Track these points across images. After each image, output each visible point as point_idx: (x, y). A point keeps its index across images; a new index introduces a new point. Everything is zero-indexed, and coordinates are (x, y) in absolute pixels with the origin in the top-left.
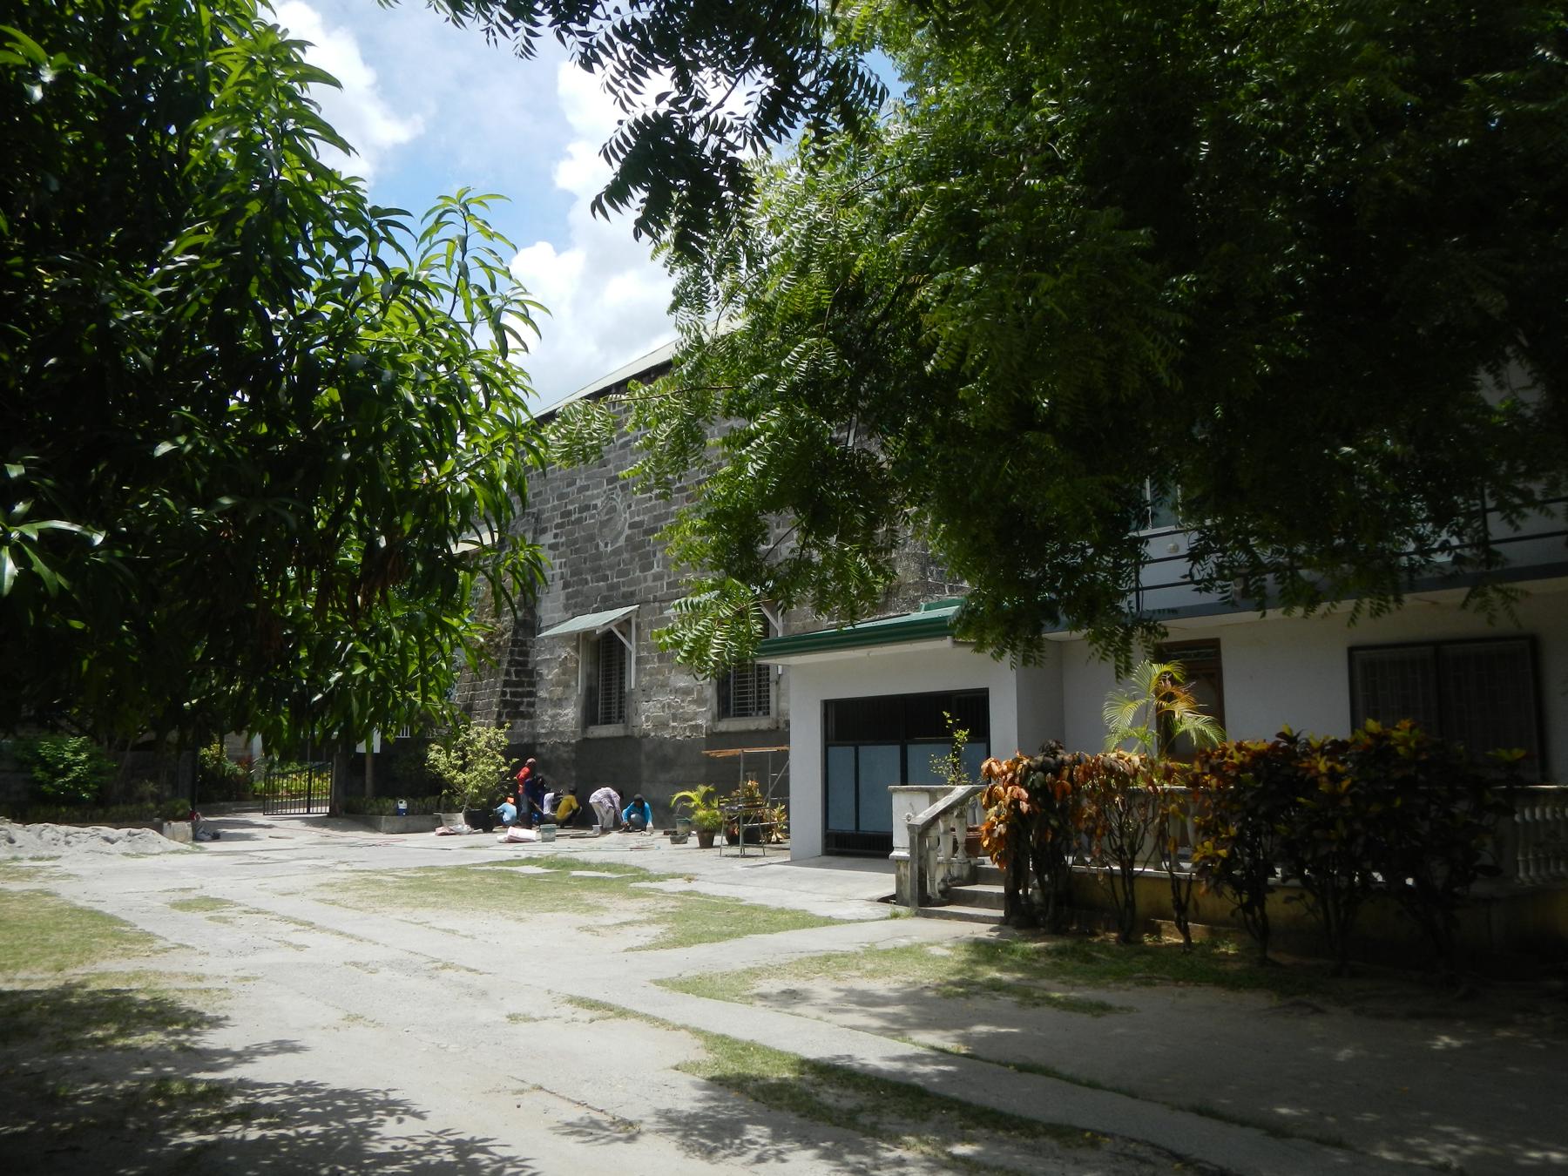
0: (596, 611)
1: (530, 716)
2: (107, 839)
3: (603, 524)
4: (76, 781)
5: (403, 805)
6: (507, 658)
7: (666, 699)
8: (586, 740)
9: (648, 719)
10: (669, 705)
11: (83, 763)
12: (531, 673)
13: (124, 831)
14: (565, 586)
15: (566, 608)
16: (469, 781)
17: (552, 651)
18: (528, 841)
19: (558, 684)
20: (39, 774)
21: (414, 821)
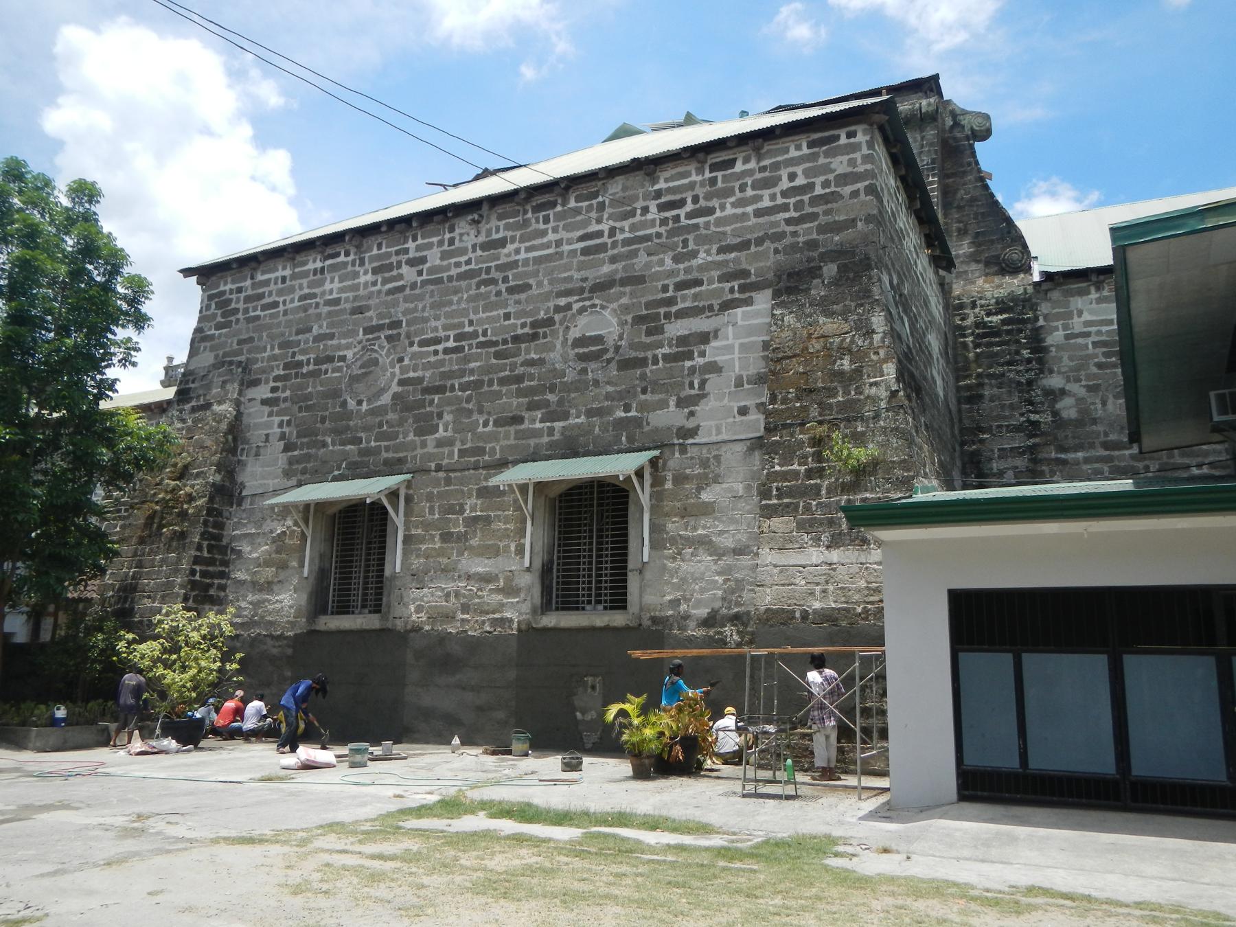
0: (335, 479)
3: (354, 379)
6: (200, 529)
7: (450, 586)
9: (419, 609)
10: (457, 594)
12: (223, 550)
14: (287, 449)
15: (287, 474)
17: (258, 524)
18: (328, 766)
19: (267, 563)
21: (75, 733)
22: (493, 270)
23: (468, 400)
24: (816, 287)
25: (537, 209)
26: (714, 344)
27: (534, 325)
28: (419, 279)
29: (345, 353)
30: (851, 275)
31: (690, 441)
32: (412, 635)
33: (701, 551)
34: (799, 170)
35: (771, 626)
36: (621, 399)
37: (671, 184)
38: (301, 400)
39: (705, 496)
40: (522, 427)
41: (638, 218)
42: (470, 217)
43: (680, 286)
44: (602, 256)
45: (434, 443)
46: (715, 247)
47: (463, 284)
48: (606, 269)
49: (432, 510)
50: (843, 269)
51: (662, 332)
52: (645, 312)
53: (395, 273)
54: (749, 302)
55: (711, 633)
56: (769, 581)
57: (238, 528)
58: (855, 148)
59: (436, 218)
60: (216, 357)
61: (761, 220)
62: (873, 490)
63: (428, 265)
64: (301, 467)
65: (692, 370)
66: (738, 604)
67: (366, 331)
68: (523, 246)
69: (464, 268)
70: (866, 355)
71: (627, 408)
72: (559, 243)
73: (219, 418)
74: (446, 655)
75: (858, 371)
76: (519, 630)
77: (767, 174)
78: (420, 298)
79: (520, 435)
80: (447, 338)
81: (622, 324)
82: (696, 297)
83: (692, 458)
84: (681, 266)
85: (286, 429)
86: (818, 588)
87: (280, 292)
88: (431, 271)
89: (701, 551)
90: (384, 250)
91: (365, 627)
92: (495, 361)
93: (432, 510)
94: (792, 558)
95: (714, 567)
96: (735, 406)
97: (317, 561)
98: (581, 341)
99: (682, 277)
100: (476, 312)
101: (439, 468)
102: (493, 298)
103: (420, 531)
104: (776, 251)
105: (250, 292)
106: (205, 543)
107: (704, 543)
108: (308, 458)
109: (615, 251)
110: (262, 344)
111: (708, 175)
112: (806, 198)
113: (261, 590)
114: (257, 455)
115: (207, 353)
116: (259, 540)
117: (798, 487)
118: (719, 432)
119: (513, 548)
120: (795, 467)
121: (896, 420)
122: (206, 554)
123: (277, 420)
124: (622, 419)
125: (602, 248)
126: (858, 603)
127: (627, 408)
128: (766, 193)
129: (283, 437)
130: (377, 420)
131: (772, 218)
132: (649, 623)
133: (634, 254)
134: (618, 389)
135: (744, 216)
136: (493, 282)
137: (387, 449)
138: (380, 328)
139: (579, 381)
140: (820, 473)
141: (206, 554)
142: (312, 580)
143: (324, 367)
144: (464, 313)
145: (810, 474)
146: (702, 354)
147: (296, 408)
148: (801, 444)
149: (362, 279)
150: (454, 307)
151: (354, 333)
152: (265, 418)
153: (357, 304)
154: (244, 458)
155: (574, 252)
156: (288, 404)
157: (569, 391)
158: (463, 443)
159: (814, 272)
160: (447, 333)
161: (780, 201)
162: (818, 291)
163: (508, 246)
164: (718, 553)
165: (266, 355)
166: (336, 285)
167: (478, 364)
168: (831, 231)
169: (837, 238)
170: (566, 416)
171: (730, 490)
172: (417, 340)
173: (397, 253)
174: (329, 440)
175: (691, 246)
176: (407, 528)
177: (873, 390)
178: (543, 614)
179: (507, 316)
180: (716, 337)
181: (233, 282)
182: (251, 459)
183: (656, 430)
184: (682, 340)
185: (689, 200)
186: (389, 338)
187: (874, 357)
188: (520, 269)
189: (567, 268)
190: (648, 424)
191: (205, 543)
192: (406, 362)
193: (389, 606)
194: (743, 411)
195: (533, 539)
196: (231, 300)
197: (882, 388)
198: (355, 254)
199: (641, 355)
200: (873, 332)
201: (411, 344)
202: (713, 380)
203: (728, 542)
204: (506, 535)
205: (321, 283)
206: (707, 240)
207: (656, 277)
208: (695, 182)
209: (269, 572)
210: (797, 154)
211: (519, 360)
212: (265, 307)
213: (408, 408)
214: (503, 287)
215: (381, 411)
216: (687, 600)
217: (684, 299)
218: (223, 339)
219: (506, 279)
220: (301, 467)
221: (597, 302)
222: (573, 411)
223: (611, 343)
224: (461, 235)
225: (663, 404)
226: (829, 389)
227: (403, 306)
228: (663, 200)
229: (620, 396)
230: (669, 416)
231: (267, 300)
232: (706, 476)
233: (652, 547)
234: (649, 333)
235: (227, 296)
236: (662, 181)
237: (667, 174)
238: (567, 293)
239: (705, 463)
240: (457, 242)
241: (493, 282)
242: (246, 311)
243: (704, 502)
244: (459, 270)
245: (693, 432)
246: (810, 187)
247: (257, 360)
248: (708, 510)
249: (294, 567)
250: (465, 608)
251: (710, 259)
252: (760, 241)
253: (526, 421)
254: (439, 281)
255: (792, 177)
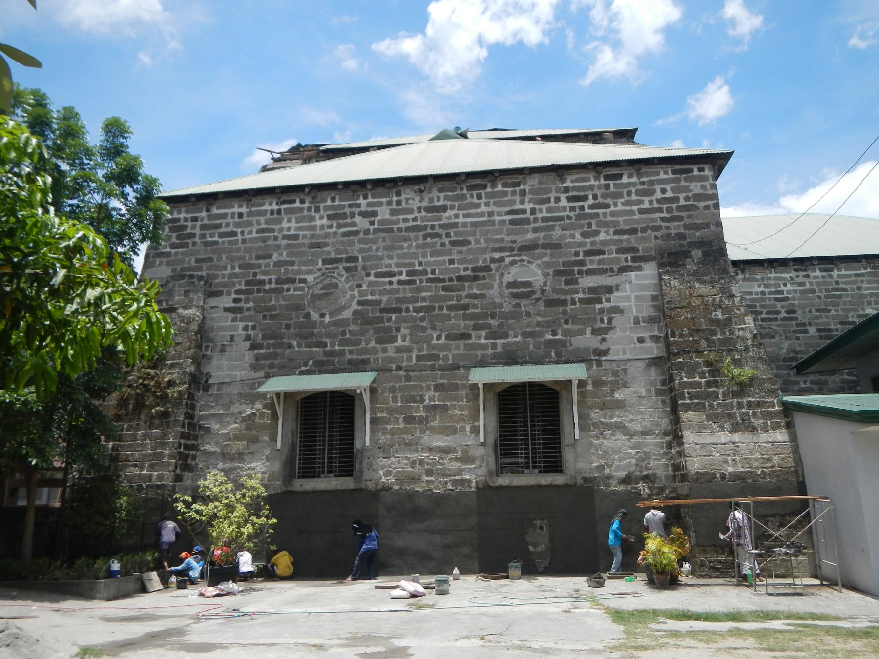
0: (302, 373)
3: (315, 298)
7: (415, 456)
10: (422, 462)
14: (253, 347)
15: (254, 367)
17: (227, 406)
19: (238, 438)
22: (437, 227)
23: (422, 319)
24: (690, 264)
25: (471, 188)
26: (616, 294)
27: (474, 269)
28: (372, 228)
29: (306, 277)
30: (712, 259)
31: (604, 358)
32: (383, 493)
33: (617, 432)
34: (668, 187)
35: (701, 483)
36: (550, 326)
37: (576, 184)
38: (266, 311)
39: (618, 396)
40: (470, 342)
41: (552, 204)
42: (417, 187)
43: (588, 253)
44: (526, 227)
45: (394, 350)
46: (612, 231)
47: (412, 235)
48: (530, 236)
49: (395, 399)
50: (705, 254)
51: (577, 284)
52: (562, 268)
53: (349, 220)
54: (639, 269)
55: (629, 488)
56: (694, 453)
57: (207, 410)
58: (705, 178)
59: (388, 185)
60: (174, 270)
61: (643, 216)
62: (753, 396)
63: (379, 218)
64: (267, 362)
65: (602, 311)
66: (647, 469)
67: (325, 262)
68: (461, 213)
69: (411, 223)
70: (732, 310)
71: (554, 333)
72: (491, 214)
73: (189, 321)
74: (412, 508)
75: (729, 320)
76: (477, 488)
77: (645, 187)
78: (375, 241)
79: (468, 347)
80: (401, 273)
81: (546, 275)
82: (600, 262)
83: (606, 370)
84: (588, 240)
85: (252, 333)
86: (729, 458)
87: (238, 225)
88: (381, 222)
89: (617, 432)
90: (337, 202)
91: (339, 487)
92: (443, 293)
93: (395, 399)
94: (707, 439)
95: (628, 444)
96: (635, 336)
97: (290, 436)
98: (513, 284)
99: (588, 247)
100: (424, 255)
101: (399, 368)
102: (439, 248)
103: (385, 415)
104: (656, 238)
105: (206, 222)
106: (186, 421)
107: (620, 427)
108: (275, 356)
109: (537, 225)
110: (222, 263)
111: (603, 182)
112: (674, 206)
113: (232, 459)
114: (223, 351)
115: (164, 267)
116: (227, 420)
117: (702, 392)
118: (624, 353)
119: (468, 428)
120: (697, 379)
121: (760, 353)
122: (187, 431)
123: (241, 325)
124: (550, 340)
125: (526, 221)
126: (757, 468)
127: (554, 333)
128: (646, 199)
129: (248, 338)
130: (340, 330)
131: (652, 216)
132: (582, 482)
133: (552, 228)
134: (547, 319)
135: (631, 212)
136: (438, 236)
137: (351, 352)
138: (339, 260)
139: (515, 312)
140: (716, 384)
141: (187, 431)
142: (286, 451)
143: (286, 286)
144: (415, 256)
145: (709, 384)
146: (608, 300)
147: (261, 316)
148: (698, 364)
149: (318, 222)
150: (404, 251)
151: (313, 262)
152: (229, 323)
153: (313, 241)
154: (209, 353)
155: (503, 222)
156: (252, 313)
157: (507, 318)
158: (419, 350)
159: (686, 254)
160: (400, 269)
161: (656, 205)
162: (691, 267)
163: (449, 211)
164: (630, 434)
165: (227, 272)
166: (293, 224)
167: (429, 294)
168: (693, 229)
169: (698, 234)
170: (506, 336)
171: (636, 392)
172: (373, 272)
173: (350, 206)
174: (295, 343)
175: (594, 227)
176: (373, 412)
177: (741, 333)
178: (497, 476)
179: (452, 262)
180: (617, 289)
181: (187, 212)
182: (216, 355)
183: (578, 349)
184: (592, 290)
185: (590, 197)
186: (347, 269)
187: (738, 312)
188: (460, 229)
189: (499, 232)
190: (571, 345)
191: (186, 421)
192: (364, 287)
193: (361, 472)
194: (641, 340)
195: (486, 420)
196: (186, 226)
197: (747, 332)
198: (311, 203)
199: (562, 297)
200: (734, 296)
201: (368, 275)
202: (617, 320)
203: (638, 428)
204: (461, 419)
205: (279, 221)
206: (606, 224)
207: (570, 245)
208: (594, 186)
209: (241, 445)
210: (665, 177)
211: (464, 294)
212: (221, 235)
213: (367, 322)
214: (447, 241)
215: (344, 323)
216: (610, 466)
217: (592, 262)
218: (179, 257)
219: (448, 235)
220: (267, 362)
221: (525, 258)
222: (511, 333)
223: (539, 288)
224: (407, 199)
225: (582, 332)
226: (711, 330)
227: (358, 246)
228: (570, 194)
229: (548, 324)
230: (587, 340)
231: (223, 230)
232: (617, 382)
233: (580, 429)
234: (567, 283)
235: (182, 222)
236: (569, 181)
237: (574, 177)
238: (501, 250)
239: (616, 373)
240: (403, 204)
241: (438, 236)
242: (203, 236)
243: (617, 400)
244: (407, 224)
245: (606, 352)
246: (675, 199)
247: (218, 276)
248: (620, 405)
249: (266, 441)
250: (429, 473)
251: (608, 237)
252: (644, 230)
253: (473, 338)
254: (391, 231)
255: (664, 191)
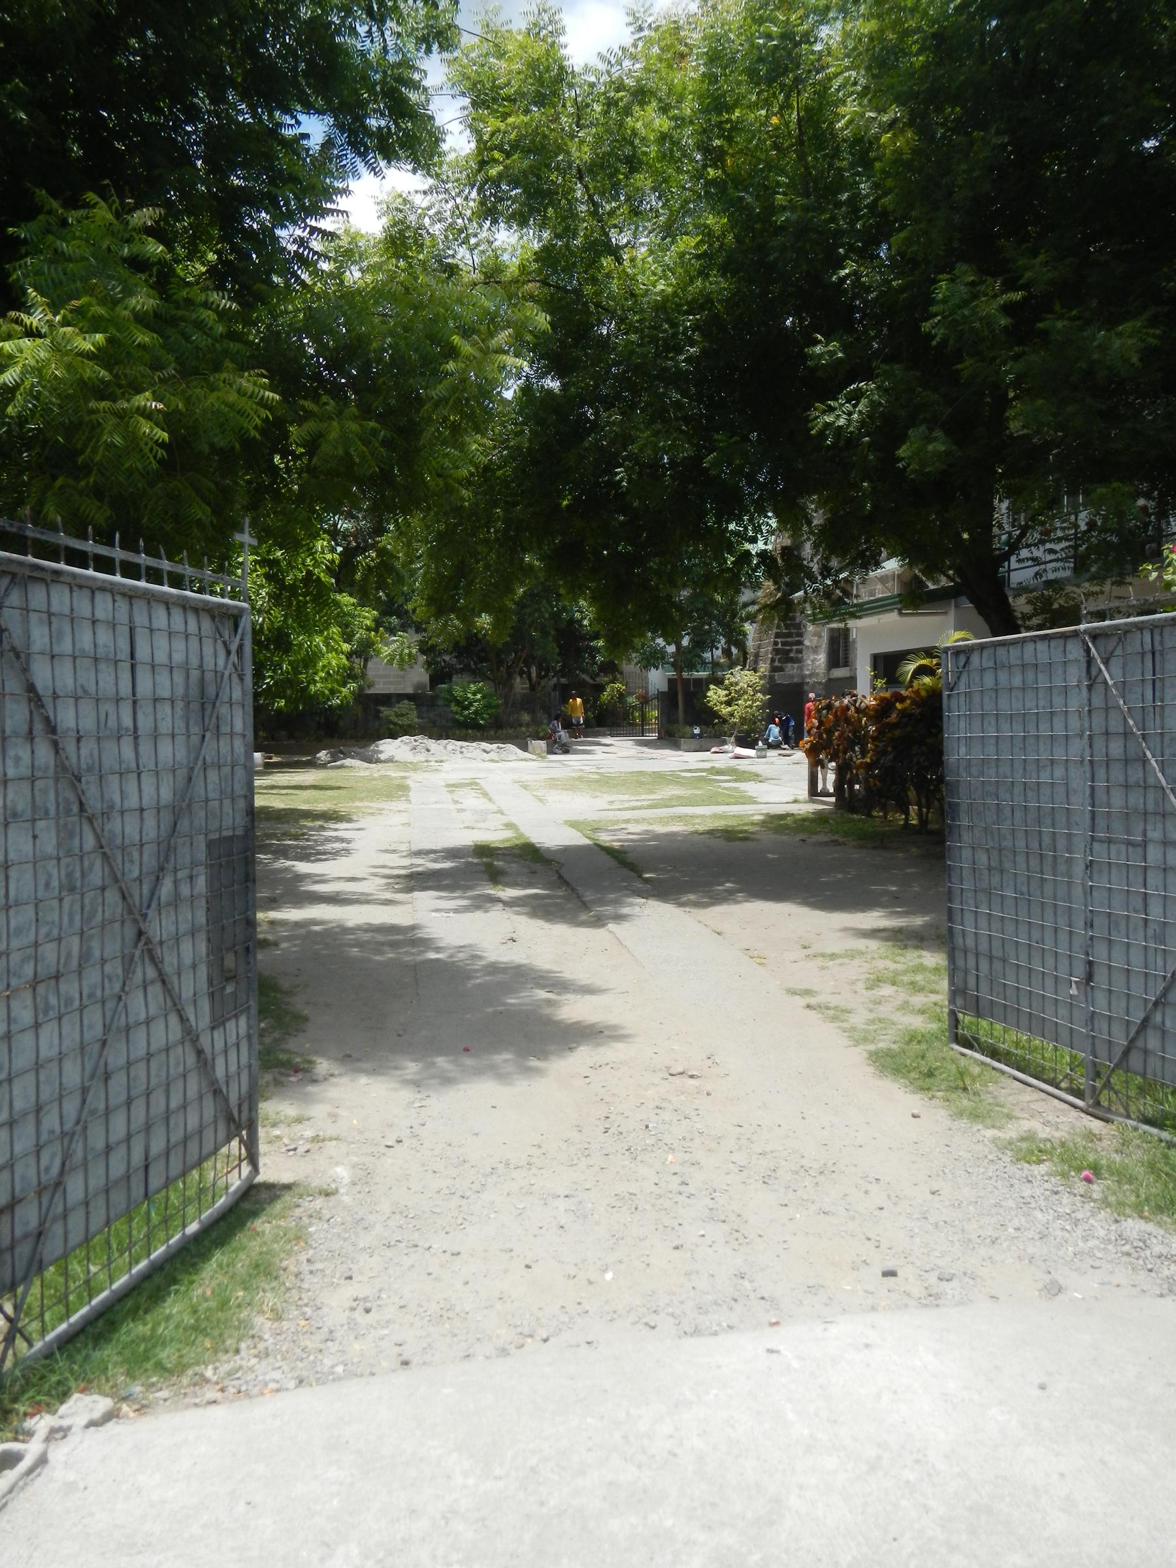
1: (799, 661)
2: (485, 751)
4: (476, 713)
5: (697, 731)
8: (830, 680)
11: (478, 701)
13: (495, 746)
16: (739, 710)
19: (814, 635)
20: (454, 708)
21: (704, 742)
